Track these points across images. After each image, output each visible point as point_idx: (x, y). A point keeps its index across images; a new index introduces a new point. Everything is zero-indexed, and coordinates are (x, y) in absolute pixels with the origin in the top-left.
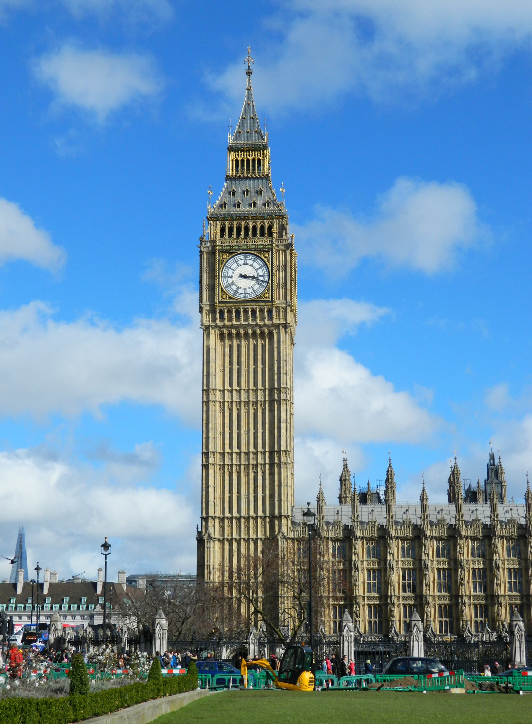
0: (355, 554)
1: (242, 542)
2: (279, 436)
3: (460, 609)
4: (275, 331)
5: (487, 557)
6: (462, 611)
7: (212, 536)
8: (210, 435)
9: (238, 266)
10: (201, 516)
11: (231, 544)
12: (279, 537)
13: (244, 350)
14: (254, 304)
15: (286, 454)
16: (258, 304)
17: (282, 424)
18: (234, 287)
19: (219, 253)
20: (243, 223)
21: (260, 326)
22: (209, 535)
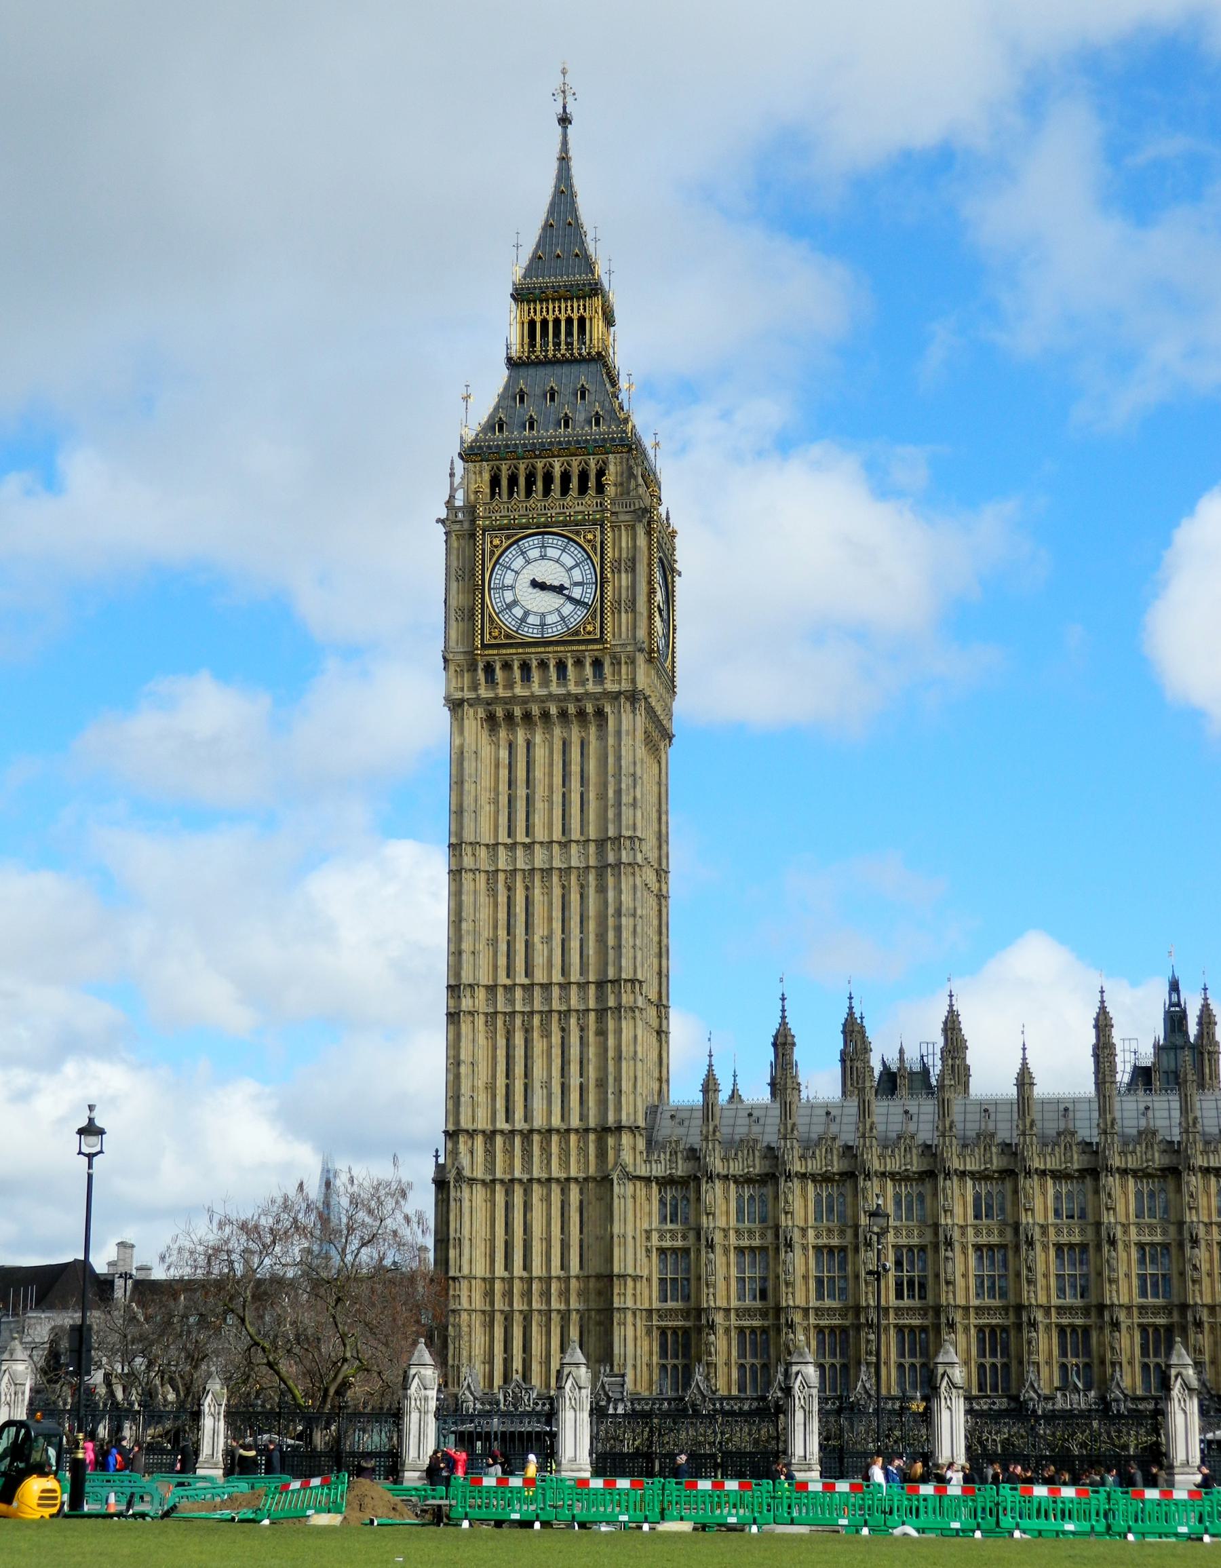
0: (786, 1213)
1: (535, 1186)
2: (618, 947)
3: (1025, 1336)
4: (608, 709)
5: (1091, 1219)
6: (1029, 1343)
7: (467, 1173)
8: (464, 946)
9: (528, 562)
10: (444, 1128)
11: (509, 1193)
13: (540, 753)
14: (562, 649)
15: (633, 987)
17: (624, 920)
19: (483, 534)
20: (540, 465)
21: (578, 698)
22: (459, 1172)
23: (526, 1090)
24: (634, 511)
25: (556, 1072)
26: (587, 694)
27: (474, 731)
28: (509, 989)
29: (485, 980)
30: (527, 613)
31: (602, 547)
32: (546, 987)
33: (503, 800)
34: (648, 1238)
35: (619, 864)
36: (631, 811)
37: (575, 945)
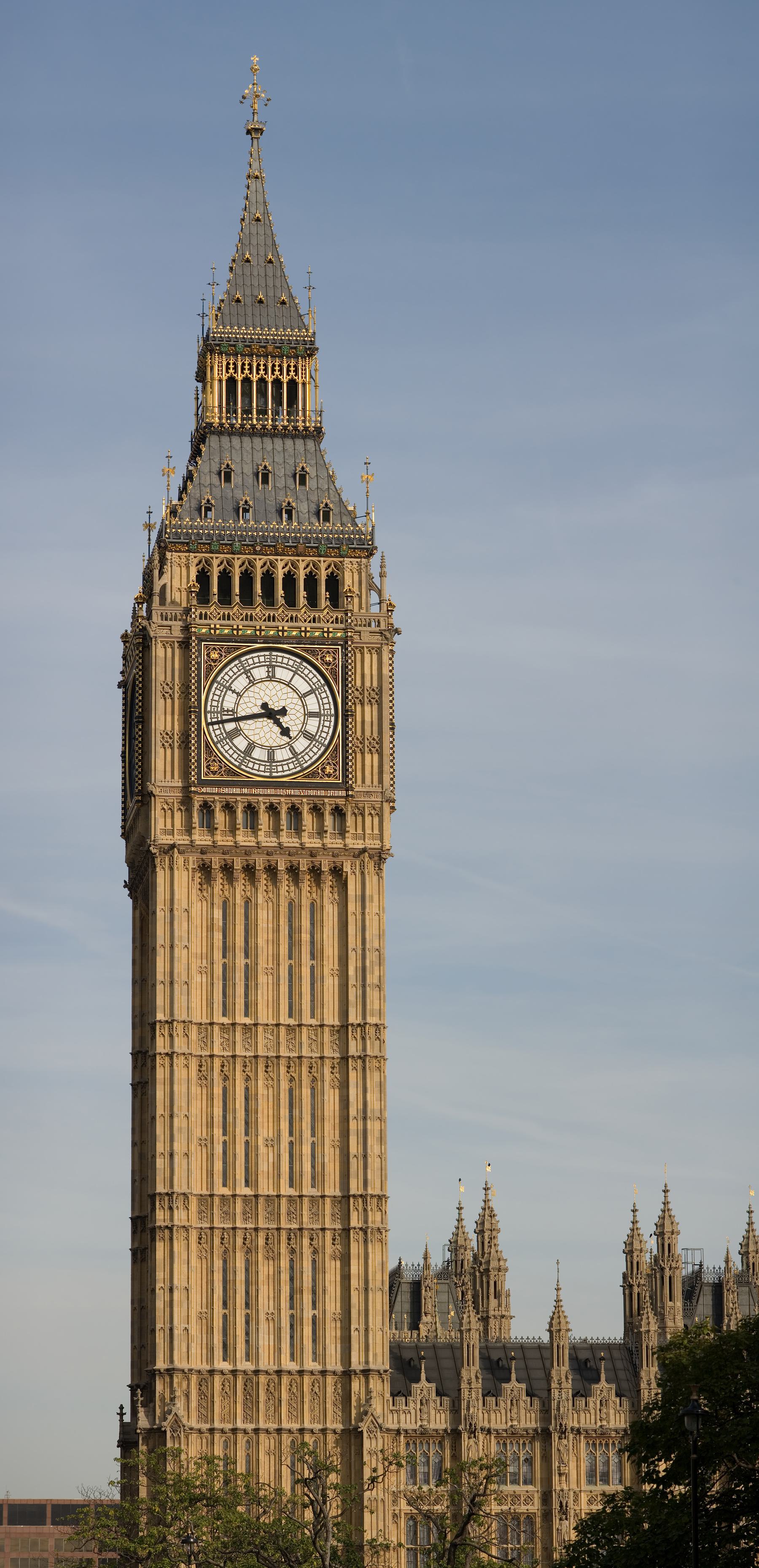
4: (347, 868)
9: (252, 682)
12: (364, 1427)
16: (306, 792)
18: (241, 743)
21: (312, 853)
23: (247, 1323)
27: (185, 884)
29: (198, 1187)
31: (345, 674)
33: (218, 970)
36: (376, 993)
37: (307, 1150)
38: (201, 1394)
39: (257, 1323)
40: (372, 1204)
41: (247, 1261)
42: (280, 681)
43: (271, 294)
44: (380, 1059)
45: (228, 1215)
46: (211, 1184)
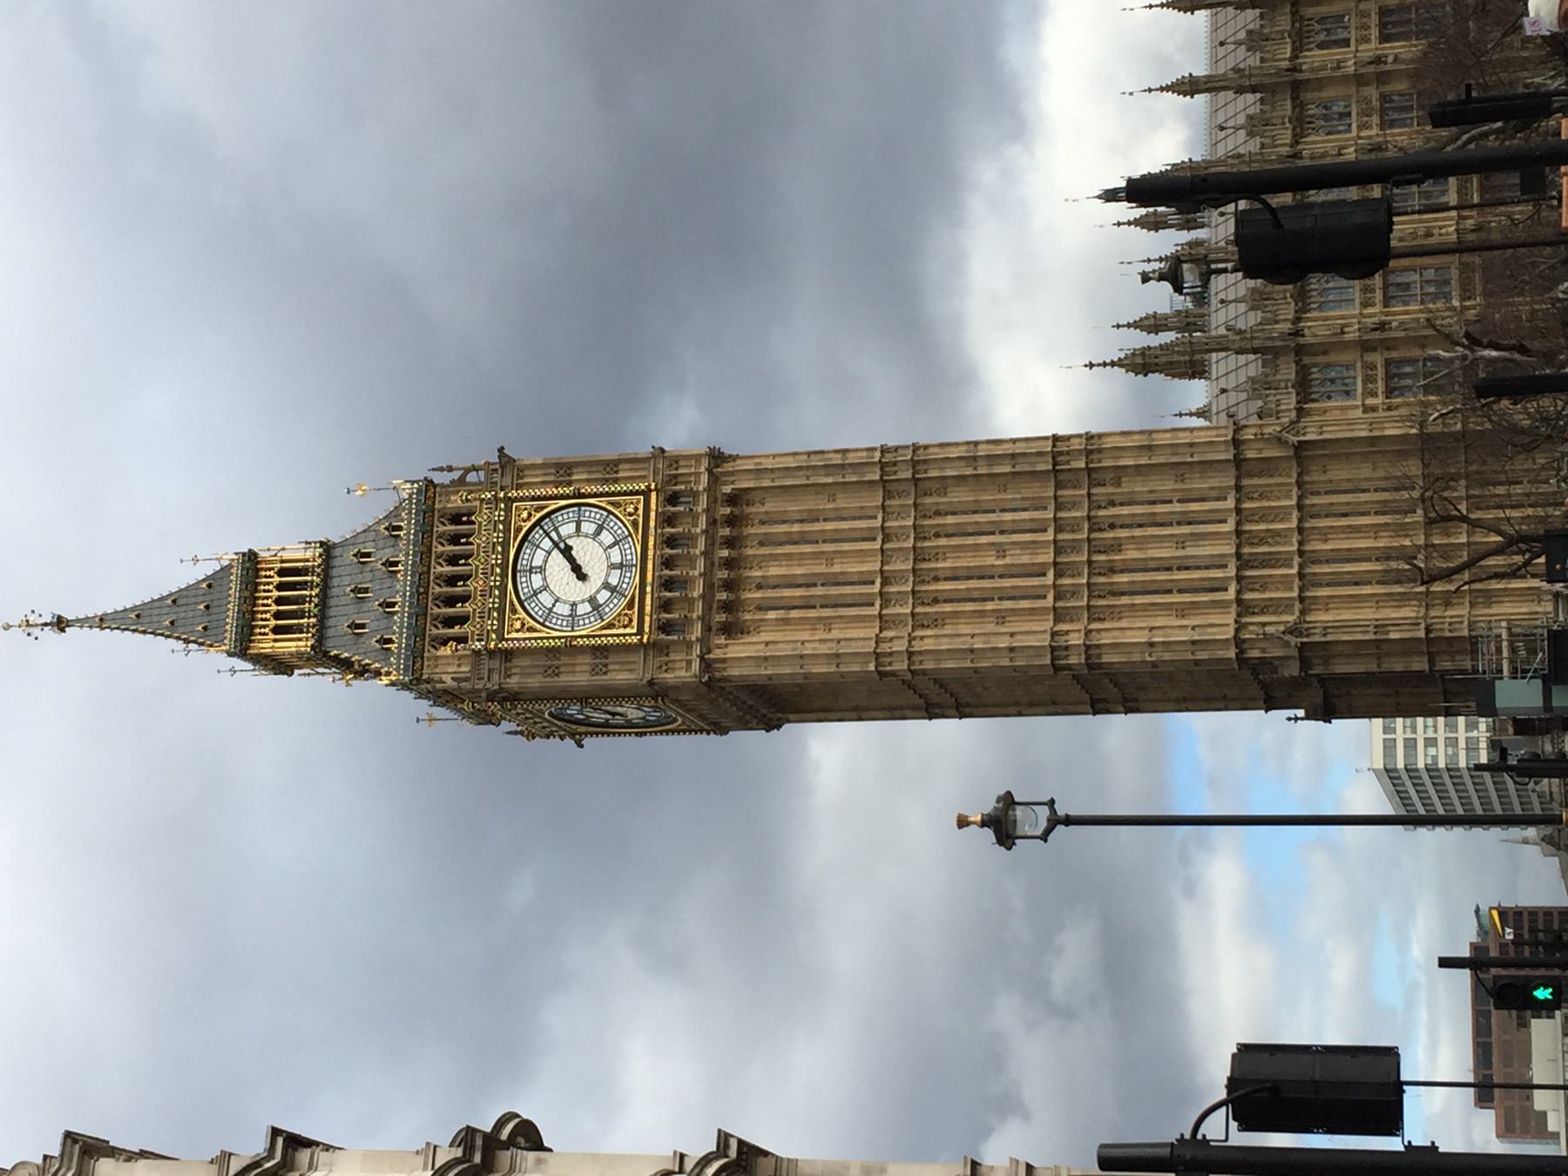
1: (1307, 548)
9: (546, 588)
16: (652, 530)
18: (603, 596)
21: (712, 523)
22: (1292, 631)
23: (1188, 568)
24: (502, 467)
25: (1167, 531)
26: (707, 511)
28: (1056, 598)
29: (1048, 624)
30: (606, 586)
32: (1058, 551)
34: (1374, 409)
35: (914, 464)
36: (850, 455)
37: (1008, 516)
38: (1262, 612)
39: (1187, 557)
40: (1062, 447)
41: (1122, 571)
42: (546, 562)
43: (201, 599)
44: (916, 448)
45: (1075, 592)
46: (1043, 611)
